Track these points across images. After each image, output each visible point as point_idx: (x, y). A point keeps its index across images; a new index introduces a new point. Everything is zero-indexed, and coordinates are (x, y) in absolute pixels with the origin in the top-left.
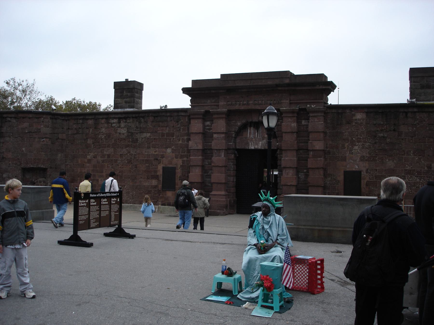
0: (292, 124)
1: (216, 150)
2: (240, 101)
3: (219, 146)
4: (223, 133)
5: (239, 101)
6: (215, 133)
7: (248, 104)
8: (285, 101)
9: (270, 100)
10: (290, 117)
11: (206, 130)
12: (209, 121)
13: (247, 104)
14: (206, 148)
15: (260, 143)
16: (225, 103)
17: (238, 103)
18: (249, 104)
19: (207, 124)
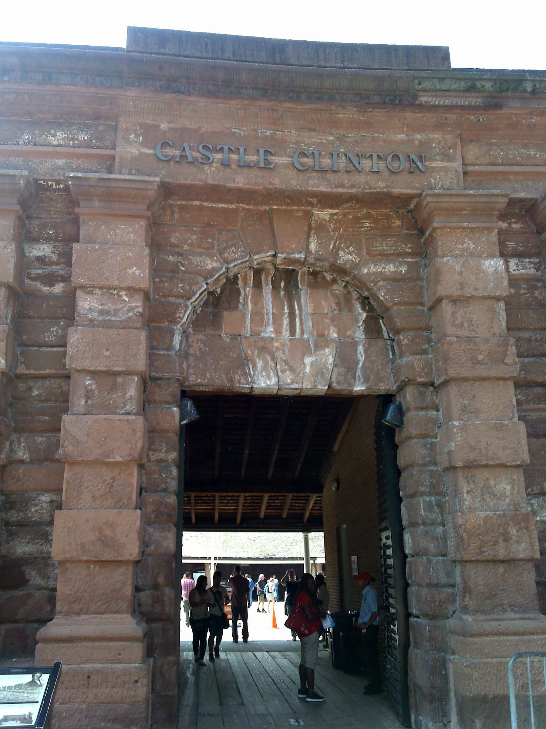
0: (487, 263)
1: (94, 374)
2: (226, 148)
3: (108, 353)
4: (131, 290)
5: (222, 150)
6: (87, 289)
7: (268, 167)
8: (439, 164)
9: (375, 156)
10: (472, 229)
11: (27, 281)
12: (48, 239)
13: (262, 165)
14: (22, 370)
15: (308, 360)
16: (151, 151)
17: (219, 156)
18: (272, 166)
19: (40, 254)
